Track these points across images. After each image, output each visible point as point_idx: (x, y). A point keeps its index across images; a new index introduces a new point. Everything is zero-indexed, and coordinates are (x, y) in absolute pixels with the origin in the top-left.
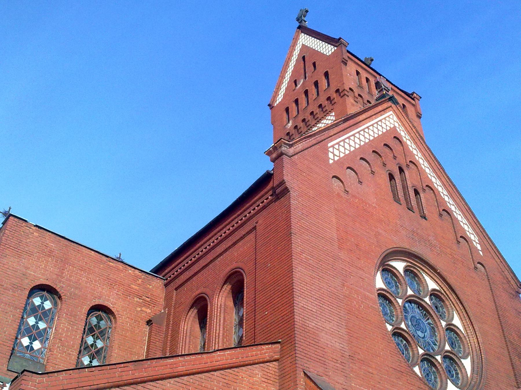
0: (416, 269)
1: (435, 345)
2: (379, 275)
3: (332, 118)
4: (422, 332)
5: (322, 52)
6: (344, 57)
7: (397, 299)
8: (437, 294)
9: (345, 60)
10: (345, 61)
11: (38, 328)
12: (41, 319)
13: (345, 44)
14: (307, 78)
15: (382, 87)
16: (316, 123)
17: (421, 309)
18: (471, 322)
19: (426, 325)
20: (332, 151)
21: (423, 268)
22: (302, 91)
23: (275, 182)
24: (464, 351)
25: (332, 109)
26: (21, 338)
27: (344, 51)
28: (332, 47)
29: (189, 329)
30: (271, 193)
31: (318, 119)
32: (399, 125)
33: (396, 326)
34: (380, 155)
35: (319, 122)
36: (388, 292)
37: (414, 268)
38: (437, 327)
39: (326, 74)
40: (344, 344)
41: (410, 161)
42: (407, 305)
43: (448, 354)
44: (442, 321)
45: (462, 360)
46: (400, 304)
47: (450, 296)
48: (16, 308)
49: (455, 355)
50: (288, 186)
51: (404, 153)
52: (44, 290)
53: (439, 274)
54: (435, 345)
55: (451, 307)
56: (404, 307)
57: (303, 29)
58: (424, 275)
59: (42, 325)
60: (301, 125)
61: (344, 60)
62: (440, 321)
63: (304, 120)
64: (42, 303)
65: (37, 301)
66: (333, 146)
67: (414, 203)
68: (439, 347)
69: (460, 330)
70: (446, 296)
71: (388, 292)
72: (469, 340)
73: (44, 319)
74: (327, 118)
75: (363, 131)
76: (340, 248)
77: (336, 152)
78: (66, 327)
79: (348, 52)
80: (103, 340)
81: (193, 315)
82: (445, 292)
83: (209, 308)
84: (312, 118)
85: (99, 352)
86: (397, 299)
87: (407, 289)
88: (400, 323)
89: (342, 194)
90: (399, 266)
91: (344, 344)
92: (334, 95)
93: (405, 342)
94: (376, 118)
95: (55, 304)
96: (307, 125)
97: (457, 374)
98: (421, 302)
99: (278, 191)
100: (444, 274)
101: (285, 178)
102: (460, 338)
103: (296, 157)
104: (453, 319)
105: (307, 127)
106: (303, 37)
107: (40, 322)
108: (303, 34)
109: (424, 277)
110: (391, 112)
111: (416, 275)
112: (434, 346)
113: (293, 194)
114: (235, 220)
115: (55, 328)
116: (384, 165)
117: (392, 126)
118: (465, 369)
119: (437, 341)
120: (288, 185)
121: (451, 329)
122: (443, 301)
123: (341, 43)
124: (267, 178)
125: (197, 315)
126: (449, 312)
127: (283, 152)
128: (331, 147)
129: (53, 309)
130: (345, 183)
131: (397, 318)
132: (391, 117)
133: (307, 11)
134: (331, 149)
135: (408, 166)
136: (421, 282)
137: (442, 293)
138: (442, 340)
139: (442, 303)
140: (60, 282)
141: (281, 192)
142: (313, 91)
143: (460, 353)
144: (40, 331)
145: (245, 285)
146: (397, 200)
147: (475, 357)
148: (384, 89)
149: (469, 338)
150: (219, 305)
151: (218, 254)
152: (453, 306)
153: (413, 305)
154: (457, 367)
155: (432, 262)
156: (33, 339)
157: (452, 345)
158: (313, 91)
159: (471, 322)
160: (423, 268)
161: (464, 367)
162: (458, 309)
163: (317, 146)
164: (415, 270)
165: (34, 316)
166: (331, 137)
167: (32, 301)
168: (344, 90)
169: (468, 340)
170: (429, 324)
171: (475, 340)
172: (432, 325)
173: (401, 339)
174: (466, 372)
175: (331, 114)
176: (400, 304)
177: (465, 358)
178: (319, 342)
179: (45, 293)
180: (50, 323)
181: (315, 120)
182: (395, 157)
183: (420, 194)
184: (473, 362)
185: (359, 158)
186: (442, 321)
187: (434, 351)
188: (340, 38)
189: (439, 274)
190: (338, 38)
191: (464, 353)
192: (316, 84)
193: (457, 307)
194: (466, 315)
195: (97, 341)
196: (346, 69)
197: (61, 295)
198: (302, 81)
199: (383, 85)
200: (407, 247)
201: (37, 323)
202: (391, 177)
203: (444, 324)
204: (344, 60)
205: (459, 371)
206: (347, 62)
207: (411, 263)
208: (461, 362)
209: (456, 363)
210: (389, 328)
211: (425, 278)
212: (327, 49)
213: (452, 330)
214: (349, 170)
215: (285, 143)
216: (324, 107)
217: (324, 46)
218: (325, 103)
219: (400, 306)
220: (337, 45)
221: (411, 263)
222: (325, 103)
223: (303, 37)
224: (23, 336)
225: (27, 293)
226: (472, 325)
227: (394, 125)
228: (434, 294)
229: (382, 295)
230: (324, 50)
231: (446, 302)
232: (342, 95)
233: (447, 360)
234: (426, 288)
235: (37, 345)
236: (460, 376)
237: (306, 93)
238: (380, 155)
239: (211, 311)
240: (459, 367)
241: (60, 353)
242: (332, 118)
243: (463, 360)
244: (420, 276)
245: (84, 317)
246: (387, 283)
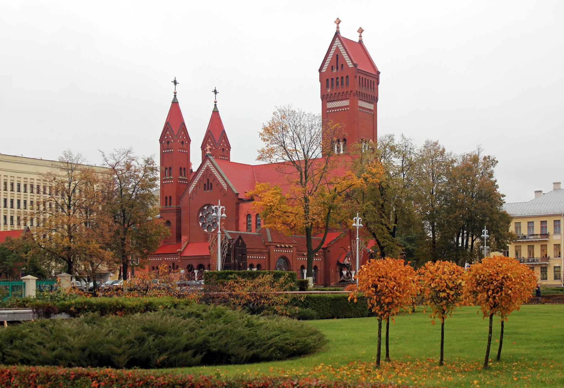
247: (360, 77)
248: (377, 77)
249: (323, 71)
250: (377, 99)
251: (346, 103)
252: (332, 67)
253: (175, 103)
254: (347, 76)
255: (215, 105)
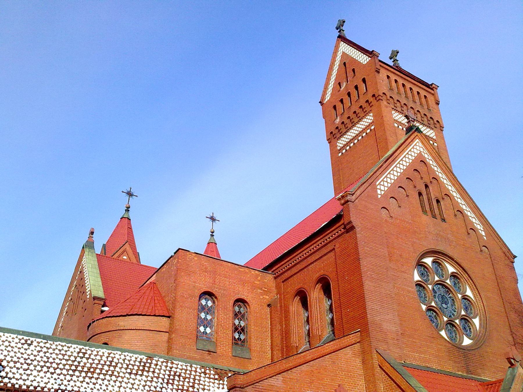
0: (440, 260)
1: (455, 311)
2: (416, 272)
3: (371, 118)
4: (446, 304)
5: (359, 60)
6: (377, 67)
7: (428, 286)
8: (455, 275)
9: (378, 69)
10: (378, 70)
11: (207, 319)
12: (208, 314)
13: (377, 55)
14: (349, 82)
15: (409, 119)
16: (359, 121)
17: (444, 288)
18: (479, 292)
19: (448, 298)
20: (379, 188)
21: (445, 259)
22: (345, 93)
23: (344, 221)
24: (475, 313)
25: (370, 111)
26: (199, 327)
27: (377, 61)
28: (367, 57)
29: (295, 310)
30: (343, 226)
31: (360, 118)
32: (423, 149)
33: (428, 305)
34: (411, 180)
35: (360, 120)
36: (422, 282)
37: (438, 260)
38: (456, 299)
39: (364, 80)
40: (397, 327)
41: (433, 178)
42: (435, 288)
43: (463, 317)
44: (458, 295)
45: (473, 319)
46: (431, 289)
47: (464, 275)
48: (194, 310)
49: (468, 317)
50: (354, 225)
51: (428, 172)
52: (206, 295)
53: (455, 261)
54: (455, 311)
55: (465, 283)
56: (433, 289)
57: (342, 38)
58: (446, 264)
59: (209, 317)
60: (347, 121)
61: (377, 70)
62: (457, 295)
63: (349, 118)
64: (207, 303)
65: (203, 302)
66: (379, 184)
67: (437, 211)
68: (457, 313)
69: (471, 298)
70: (461, 275)
71: (422, 282)
72: (478, 305)
73: (209, 313)
74: (367, 117)
75: (399, 164)
76: (390, 260)
77: (382, 188)
78: (223, 317)
79: (380, 61)
80: (244, 321)
81: (297, 301)
82: (460, 273)
83: (308, 299)
84: (355, 116)
85: (243, 330)
86: (428, 286)
87: (434, 277)
88: (431, 303)
89: (388, 219)
90: (429, 261)
91: (397, 327)
92: (371, 99)
93: (435, 314)
94: (407, 150)
95: (214, 302)
96: (352, 122)
97: (470, 329)
98: (444, 283)
99: (348, 227)
100: (459, 261)
101: (352, 219)
102: (472, 304)
103: (357, 201)
104: (466, 291)
105: (352, 123)
106: (343, 45)
107: (207, 315)
108: (342, 43)
109: (445, 265)
110: (417, 140)
111: (440, 264)
112: (454, 313)
113: (358, 229)
114: (319, 242)
115: (217, 318)
116: (415, 187)
117: (419, 152)
118: (475, 326)
119: (456, 309)
120: (354, 224)
121: (465, 298)
122: (459, 279)
123: (374, 55)
124: (339, 217)
125: (300, 301)
126: (463, 286)
127: (349, 200)
128: (378, 185)
129: (213, 306)
130: (389, 211)
131: (429, 299)
132: (417, 144)
133: (344, 22)
134: (378, 187)
135: (431, 182)
136: (443, 268)
137: (458, 274)
138: (459, 307)
139: (459, 280)
140: (214, 288)
141: (350, 228)
142: (354, 93)
143: (472, 314)
144: (209, 321)
145: (332, 288)
146: (424, 211)
147: (482, 316)
148: (411, 121)
149: (477, 303)
150: (315, 297)
151: (309, 263)
152: (466, 282)
153: (439, 286)
154: (470, 325)
155: (450, 254)
156: (206, 327)
157: (466, 309)
158: (354, 93)
159: (479, 292)
160: (445, 259)
161: (475, 324)
162: (470, 284)
163: (370, 187)
164: (439, 261)
165: (204, 312)
166: (377, 178)
167: (201, 303)
168: (379, 95)
169: (477, 304)
170: (450, 297)
171: (482, 304)
172: (452, 298)
173: (432, 312)
174: (476, 327)
175: (370, 115)
176: (431, 289)
177: (475, 317)
178: (383, 329)
179: (207, 296)
180: (213, 314)
181: (358, 118)
182: (422, 178)
183: (441, 203)
184: (481, 319)
185: (397, 187)
186: (458, 295)
187: (454, 316)
188: (373, 51)
189: (455, 261)
190: (371, 51)
191: (474, 313)
192: (356, 87)
193: (469, 283)
194: (475, 288)
195: (241, 322)
196: (379, 76)
197: (217, 296)
198: (345, 84)
199: (410, 118)
200: (434, 247)
201: (206, 316)
202: (420, 194)
203: (460, 296)
204: (377, 70)
205: (471, 327)
206: (379, 71)
207: (436, 257)
208: (472, 321)
209: (469, 322)
210: (424, 307)
211: (447, 266)
212: (364, 59)
213: (465, 299)
214: (392, 199)
215: (349, 194)
216: (364, 108)
217: (360, 56)
218: (365, 105)
219: (430, 290)
220: (370, 56)
221: (436, 257)
222: (365, 105)
223: (343, 45)
224: (200, 326)
225: (198, 298)
226: (479, 294)
227: (420, 151)
228: (454, 276)
229: (419, 285)
230: (361, 59)
231: (461, 280)
232: (377, 99)
233: (463, 321)
234: (447, 272)
235: (208, 330)
236: (472, 330)
237: (349, 94)
238: (411, 180)
239: (310, 302)
240: (471, 324)
241: (222, 334)
242: (371, 118)
243: (473, 320)
244: (442, 264)
245: (231, 308)
246: (422, 275)
247: (388, 77)
248: (432, 92)
249: (328, 97)
250: (441, 128)
251: (369, 119)
252: (339, 84)
253: (126, 220)
254: (364, 80)
255: (212, 235)
